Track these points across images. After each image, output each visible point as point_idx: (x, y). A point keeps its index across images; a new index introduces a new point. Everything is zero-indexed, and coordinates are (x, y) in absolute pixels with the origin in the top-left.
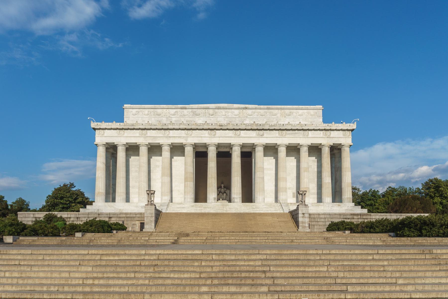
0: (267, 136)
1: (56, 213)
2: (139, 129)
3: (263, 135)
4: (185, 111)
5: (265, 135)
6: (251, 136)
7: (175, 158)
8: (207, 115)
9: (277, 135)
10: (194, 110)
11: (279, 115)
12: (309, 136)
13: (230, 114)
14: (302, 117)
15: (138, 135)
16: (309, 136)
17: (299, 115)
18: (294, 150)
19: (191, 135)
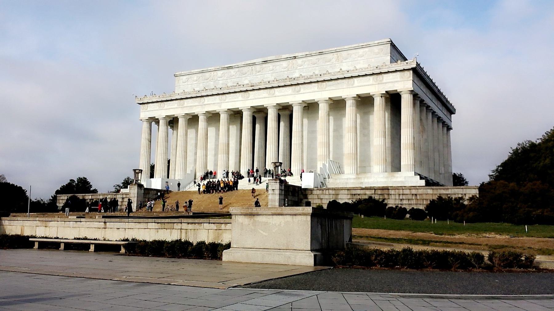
0: (305, 91)
1: (77, 195)
2: (177, 99)
3: (300, 91)
4: (232, 71)
5: (302, 91)
6: (287, 93)
7: (189, 131)
8: (254, 72)
9: (316, 89)
10: (241, 69)
11: (334, 60)
12: (354, 86)
13: (278, 67)
14: (363, 58)
15: (176, 106)
16: (354, 86)
17: (362, 56)
18: (337, 105)
19: (225, 100)
